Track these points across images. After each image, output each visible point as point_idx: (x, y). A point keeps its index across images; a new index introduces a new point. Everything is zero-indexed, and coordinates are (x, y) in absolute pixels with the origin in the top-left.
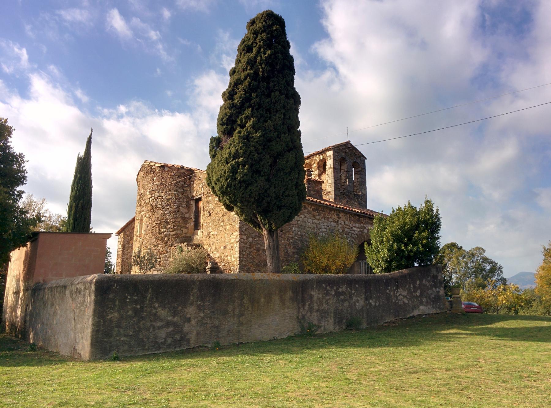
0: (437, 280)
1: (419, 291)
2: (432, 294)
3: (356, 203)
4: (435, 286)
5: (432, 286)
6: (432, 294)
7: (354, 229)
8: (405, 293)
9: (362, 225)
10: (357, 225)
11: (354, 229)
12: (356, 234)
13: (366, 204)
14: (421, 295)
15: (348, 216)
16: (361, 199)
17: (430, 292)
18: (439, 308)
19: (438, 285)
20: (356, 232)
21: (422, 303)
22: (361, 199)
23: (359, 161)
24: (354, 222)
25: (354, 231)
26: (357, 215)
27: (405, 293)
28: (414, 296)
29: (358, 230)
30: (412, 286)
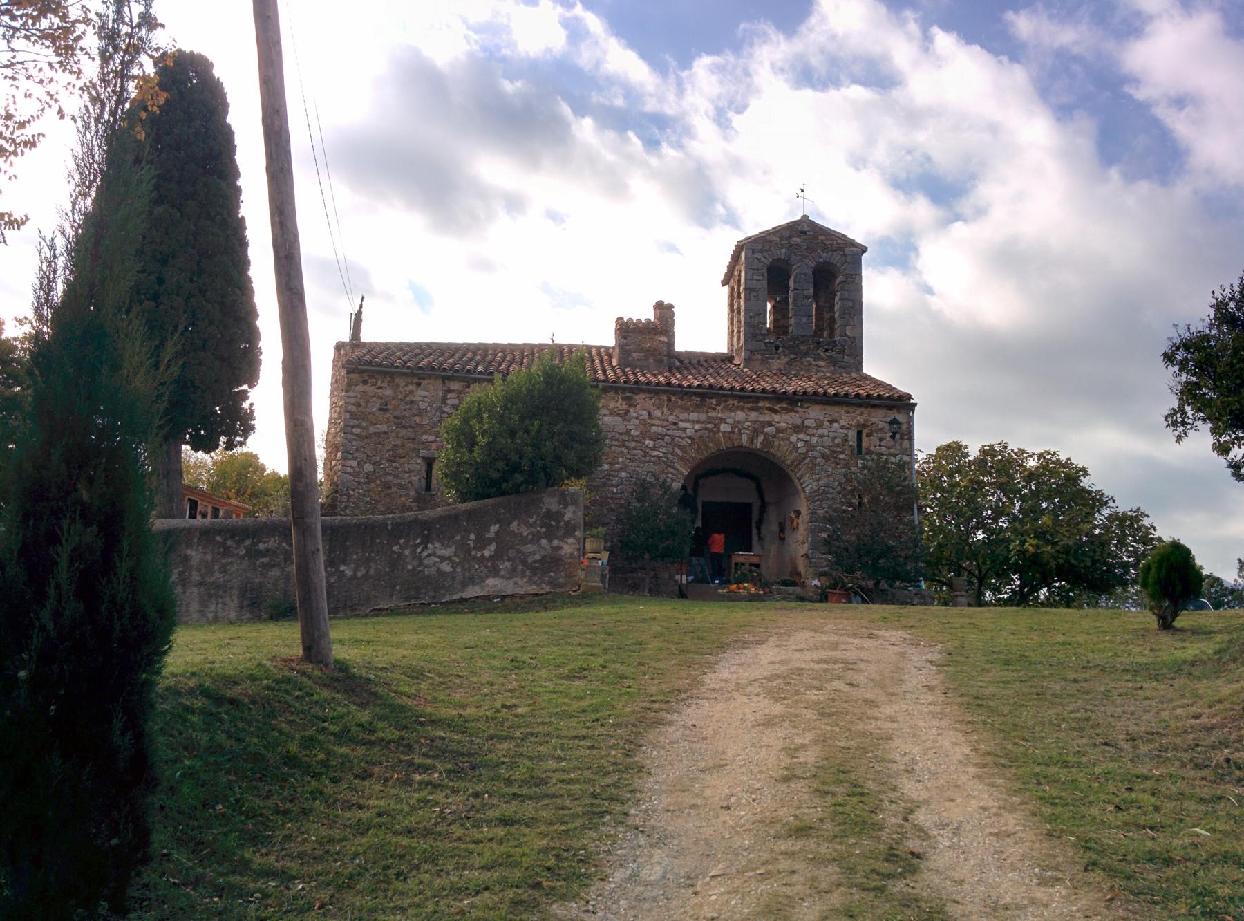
0: (558, 522)
1: (493, 547)
2: (534, 553)
3: (821, 363)
4: (550, 536)
5: (536, 538)
6: (534, 553)
7: (682, 425)
8: (448, 552)
9: (712, 414)
10: (694, 416)
11: (682, 425)
12: (690, 438)
13: (861, 361)
14: (497, 556)
15: (664, 397)
16: (842, 352)
17: (529, 548)
18: (550, 583)
19: (561, 533)
20: (689, 432)
21: (494, 572)
22: (842, 352)
23: (836, 258)
24: (685, 409)
25: (684, 430)
26: (695, 394)
27: (448, 552)
28: (475, 558)
29: (697, 427)
30: (472, 536)
